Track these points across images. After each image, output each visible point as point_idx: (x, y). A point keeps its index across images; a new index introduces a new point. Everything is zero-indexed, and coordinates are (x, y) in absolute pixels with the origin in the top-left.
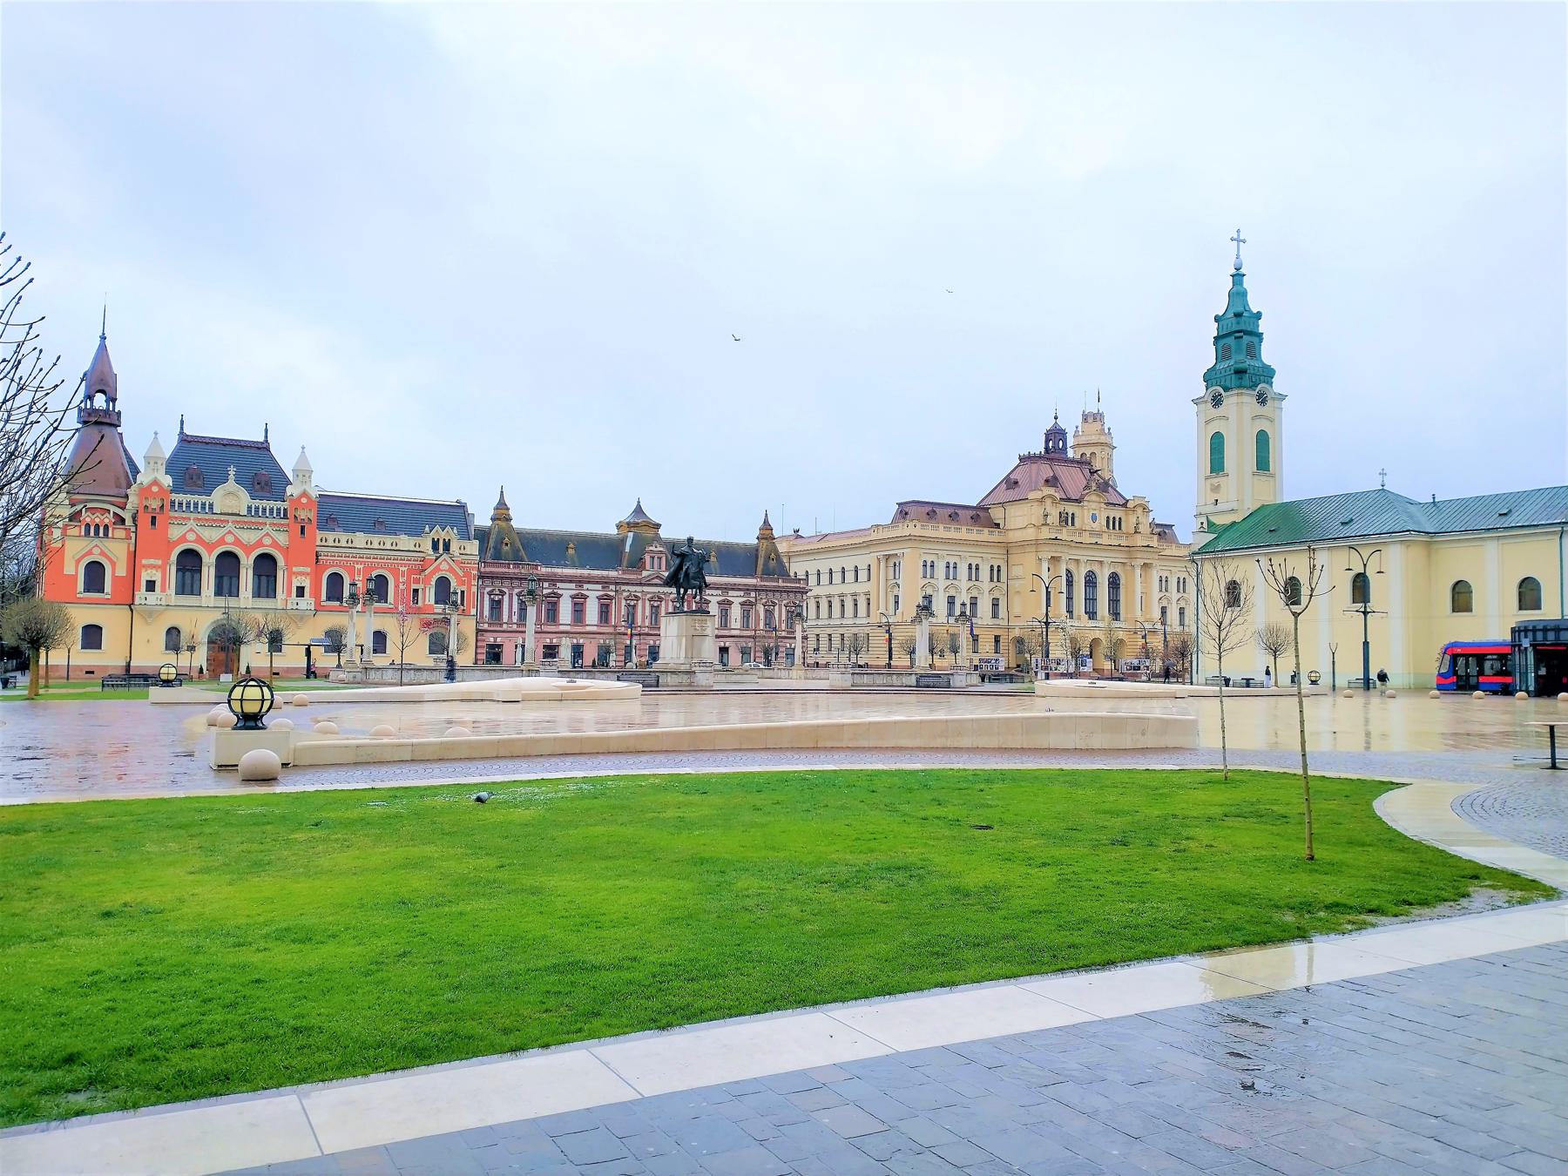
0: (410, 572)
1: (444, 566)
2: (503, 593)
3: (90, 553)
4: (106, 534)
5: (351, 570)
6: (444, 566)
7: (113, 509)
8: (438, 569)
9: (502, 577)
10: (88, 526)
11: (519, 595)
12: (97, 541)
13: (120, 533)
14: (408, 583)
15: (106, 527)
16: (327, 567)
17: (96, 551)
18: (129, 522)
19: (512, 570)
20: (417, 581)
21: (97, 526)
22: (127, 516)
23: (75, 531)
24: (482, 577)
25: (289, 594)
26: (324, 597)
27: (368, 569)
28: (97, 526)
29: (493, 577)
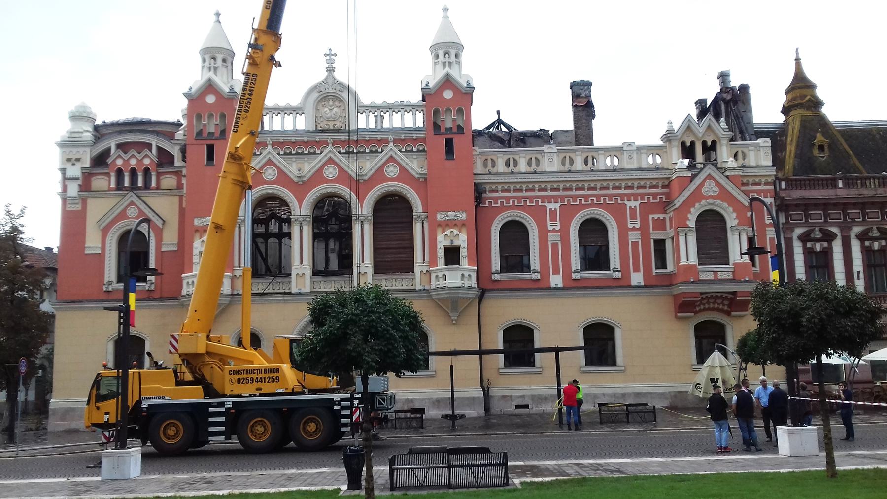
0: (646, 209)
1: (710, 189)
2: (829, 237)
3: (122, 215)
4: (147, 186)
5: (539, 213)
6: (710, 189)
7: (154, 141)
8: (697, 196)
9: (825, 205)
10: (120, 173)
11: (804, 239)
12: (132, 197)
13: (169, 181)
14: (644, 230)
15: (147, 171)
16: (503, 209)
17: (132, 212)
18: (178, 162)
19: (841, 191)
20: (660, 225)
21: (133, 173)
22: (176, 151)
23: (99, 183)
24: (783, 206)
25: (433, 262)
26: (496, 264)
27: (568, 212)
28: (133, 173)
29: (806, 206)
